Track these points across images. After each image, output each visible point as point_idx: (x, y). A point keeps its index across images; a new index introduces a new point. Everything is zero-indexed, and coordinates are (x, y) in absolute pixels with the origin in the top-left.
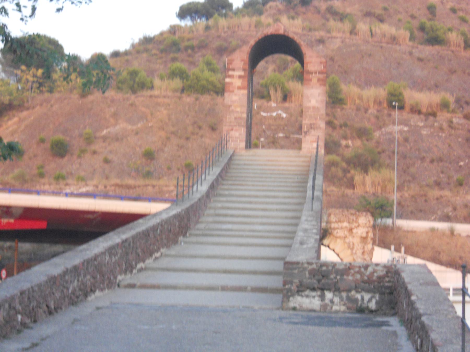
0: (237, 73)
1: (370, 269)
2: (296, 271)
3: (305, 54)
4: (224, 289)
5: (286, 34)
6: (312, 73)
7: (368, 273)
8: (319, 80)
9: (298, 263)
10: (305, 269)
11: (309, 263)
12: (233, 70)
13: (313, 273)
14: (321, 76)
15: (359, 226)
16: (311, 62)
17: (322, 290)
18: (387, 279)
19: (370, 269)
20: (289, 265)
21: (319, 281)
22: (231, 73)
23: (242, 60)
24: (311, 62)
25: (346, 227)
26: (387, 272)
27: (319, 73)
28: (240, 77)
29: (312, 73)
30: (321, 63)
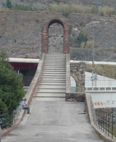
4: (53, 97)
6: (66, 31)
8: (68, 33)
12: (44, 30)
13: (71, 95)
14: (68, 32)
15: (80, 68)
16: (65, 28)
20: (67, 94)
22: (43, 31)
23: (46, 27)
24: (65, 28)
27: (68, 31)
28: (46, 32)
29: (66, 31)
30: (69, 28)
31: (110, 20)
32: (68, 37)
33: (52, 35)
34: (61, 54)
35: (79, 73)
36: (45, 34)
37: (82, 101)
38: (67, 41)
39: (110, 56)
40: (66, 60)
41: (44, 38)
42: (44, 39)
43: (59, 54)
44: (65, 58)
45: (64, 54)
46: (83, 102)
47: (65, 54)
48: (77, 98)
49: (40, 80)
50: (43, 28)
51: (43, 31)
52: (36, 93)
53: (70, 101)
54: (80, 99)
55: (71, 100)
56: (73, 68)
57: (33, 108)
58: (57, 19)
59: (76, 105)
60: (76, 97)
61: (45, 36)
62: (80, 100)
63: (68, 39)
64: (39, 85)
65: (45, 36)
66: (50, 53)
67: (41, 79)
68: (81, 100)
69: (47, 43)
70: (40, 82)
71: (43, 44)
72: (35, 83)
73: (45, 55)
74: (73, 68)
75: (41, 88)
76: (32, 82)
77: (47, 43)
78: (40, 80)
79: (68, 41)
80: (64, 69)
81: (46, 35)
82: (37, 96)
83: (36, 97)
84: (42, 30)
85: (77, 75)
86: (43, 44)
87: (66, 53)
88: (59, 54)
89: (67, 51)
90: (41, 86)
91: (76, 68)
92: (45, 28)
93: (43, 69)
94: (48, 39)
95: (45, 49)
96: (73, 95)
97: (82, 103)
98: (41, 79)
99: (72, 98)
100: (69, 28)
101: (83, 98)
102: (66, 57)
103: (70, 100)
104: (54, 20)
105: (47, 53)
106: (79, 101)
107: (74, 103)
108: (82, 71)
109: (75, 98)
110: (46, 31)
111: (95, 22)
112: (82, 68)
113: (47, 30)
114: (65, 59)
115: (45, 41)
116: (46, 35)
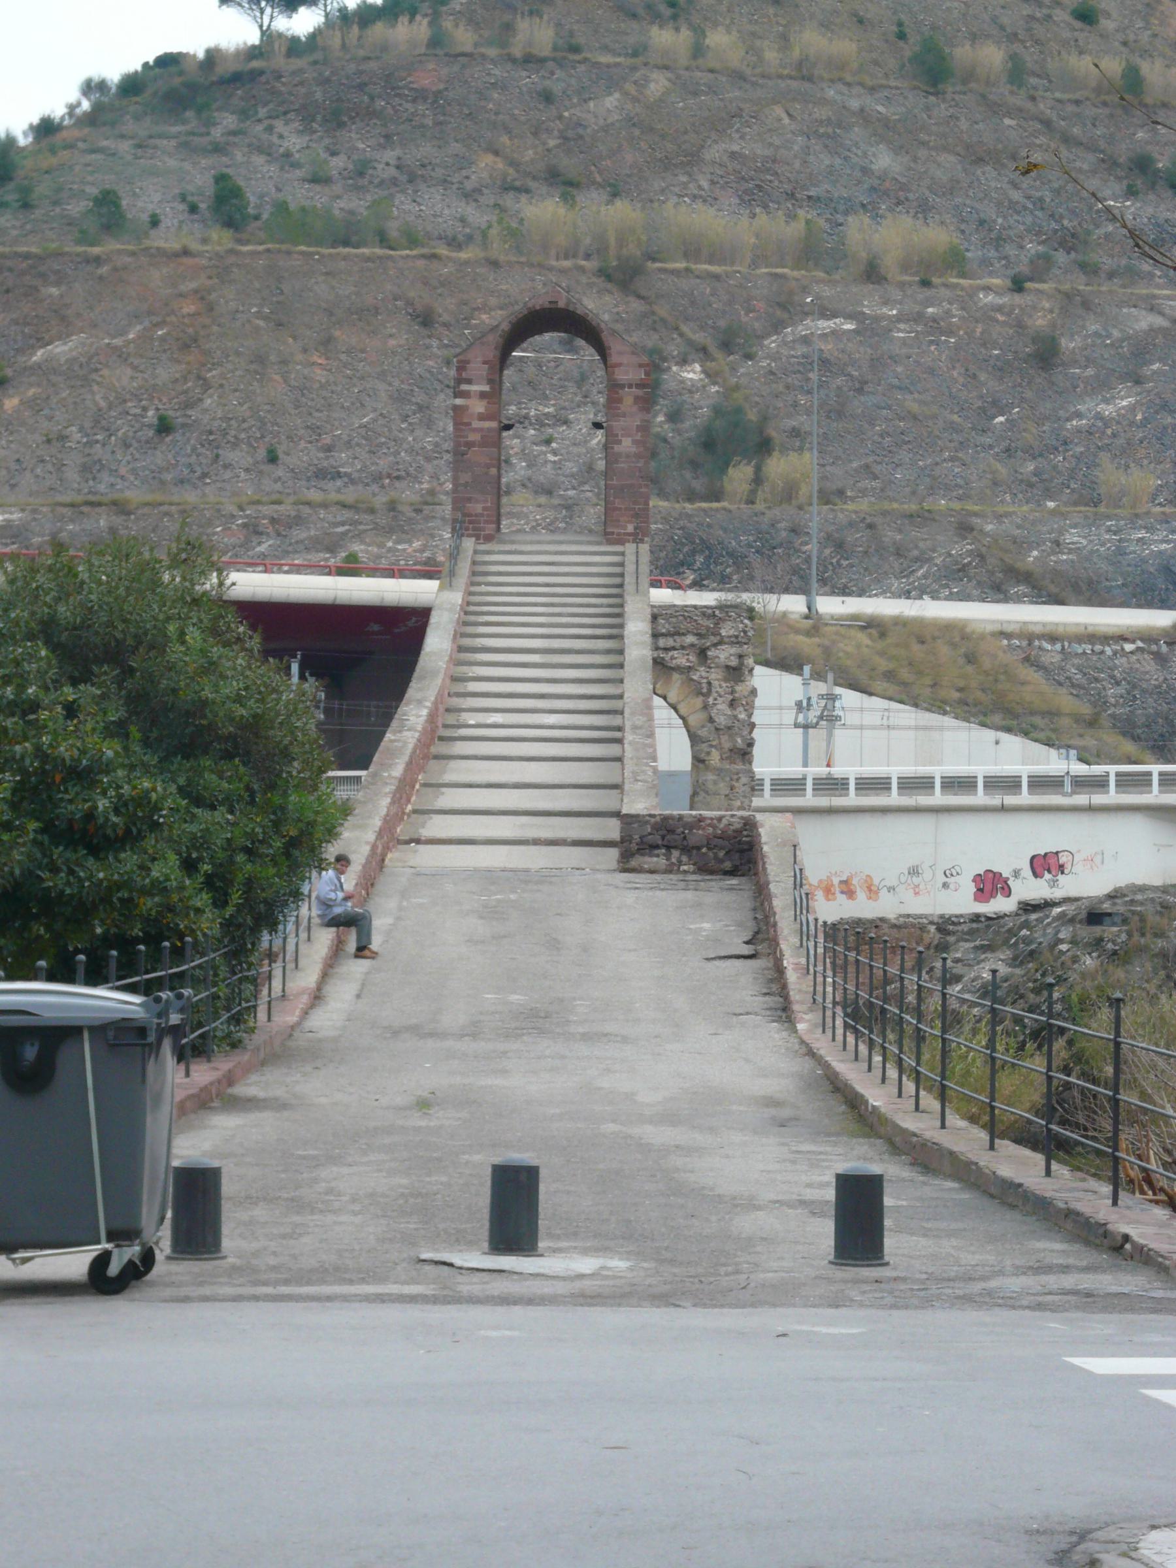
0: (475, 388)
1: (724, 821)
2: (635, 825)
3: (610, 348)
4: (536, 842)
5: (571, 308)
6: (622, 386)
7: (722, 826)
8: (637, 399)
9: (637, 816)
10: (647, 822)
11: (651, 816)
13: (657, 827)
14: (640, 392)
15: (720, 643)
16: (620, 365)
17: (668, 848)
18: (745, 833)
19: (724, 821)
20: (628, 820)
21: (663, 837)
22: (464, 387)
23: (485, 363)
24: (620, 365)
25: (692, 645)
26: (745, 824)
27: (638, 386)
28: (483, 395)
29: (622, 386)
31: (930, 310)
32: (639, 428)
33: (526, 417)
34: (589, 543)
35: (715, 676)
36: (479, 407)
37: (732, 873)
38: (628, 456)
39: (930, 560)
40: (621, 586)
41: (473, 437)
42: (470, 445)
43: (574, 548)
44: (617, 570)
45: (610, 542)
46: (743, 879)
47: (619, 548)
48: (699, 848)
49: (446, 726)
50: (461, 367)
51: (464, 387)
52: (415, 811)
53: (652, 872)
54: (721, 854)
55: (659, 861)
56: (670, 642)
57: (398, 918)
59: (690, 895)
60: (692, 841)
61: (476, 424)
62: (721, 861)
63: (635, 442)
64: (437, 757)
65: (476, 424)
66: (513, 542)
67: (451, 719)
68: (728, 865)
69: (488, 466)
70: (441, 739)
71: (465, 477)
72: (405, 743)
73: (476, 552)
74: (670, 642)
75: (449, 777)
76: (389, 736)
77: (488, 466)
78: (446, 726)
79: (638, 456)
80: (608, 652)
81: (482, 417)
82: (426, 833)
83: (418, 841)
84: (459, 381)
85: (699, 693)
86: (465, 477)
87: (621, 542)
88: (574, 548)
89: (630, 528)
90: (453, 764)
91: (690, 639)
92: (478, 367)
93: (461, 649)
94: (498, 443)
95: (478, 508)
96: (671, 831)
97: (734, 881)
98: (451, 719)
99: (668, 848)
100: (640, 366)
101: (742, 851)
102: (622, 565)
103: (649, 861)
104: (543, 310)
105: (489, 539)
106: (712, 872)
107: (682, 884)
108: (734, 662)
109: (686, 850)
110: (486, 388)
111: (822, 324)
112: (736, 641)
113: (490, 382)
114: (617, 580)
115: (477, 456)
116: (482, 417)
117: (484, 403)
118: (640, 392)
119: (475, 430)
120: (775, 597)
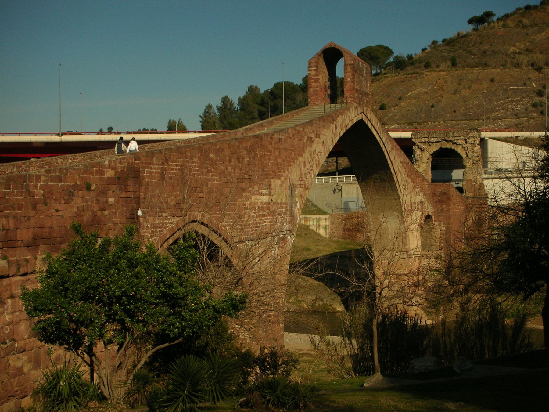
0: (313, 69)
6: (347, 65)
12: (311, 67)
14: (352, 66)
22: (310, 69)
28: (314, 70)
29: (347, 65)
30: (352, 60)
33: (513, 100)
35: (469, 146)
51: (310, 69)
56: (458, 138)
58: (333, 46)
74: (458, 138)
81: (314, 76)
85: (465, 150)
91: (462, 137)
108: (473, 142)
110: (315, 68)
112: (473, 137)
116: (314, 76)
117: (315, 72)
118: (352, 66)
119: (314, 79)
120: (533, 133)
